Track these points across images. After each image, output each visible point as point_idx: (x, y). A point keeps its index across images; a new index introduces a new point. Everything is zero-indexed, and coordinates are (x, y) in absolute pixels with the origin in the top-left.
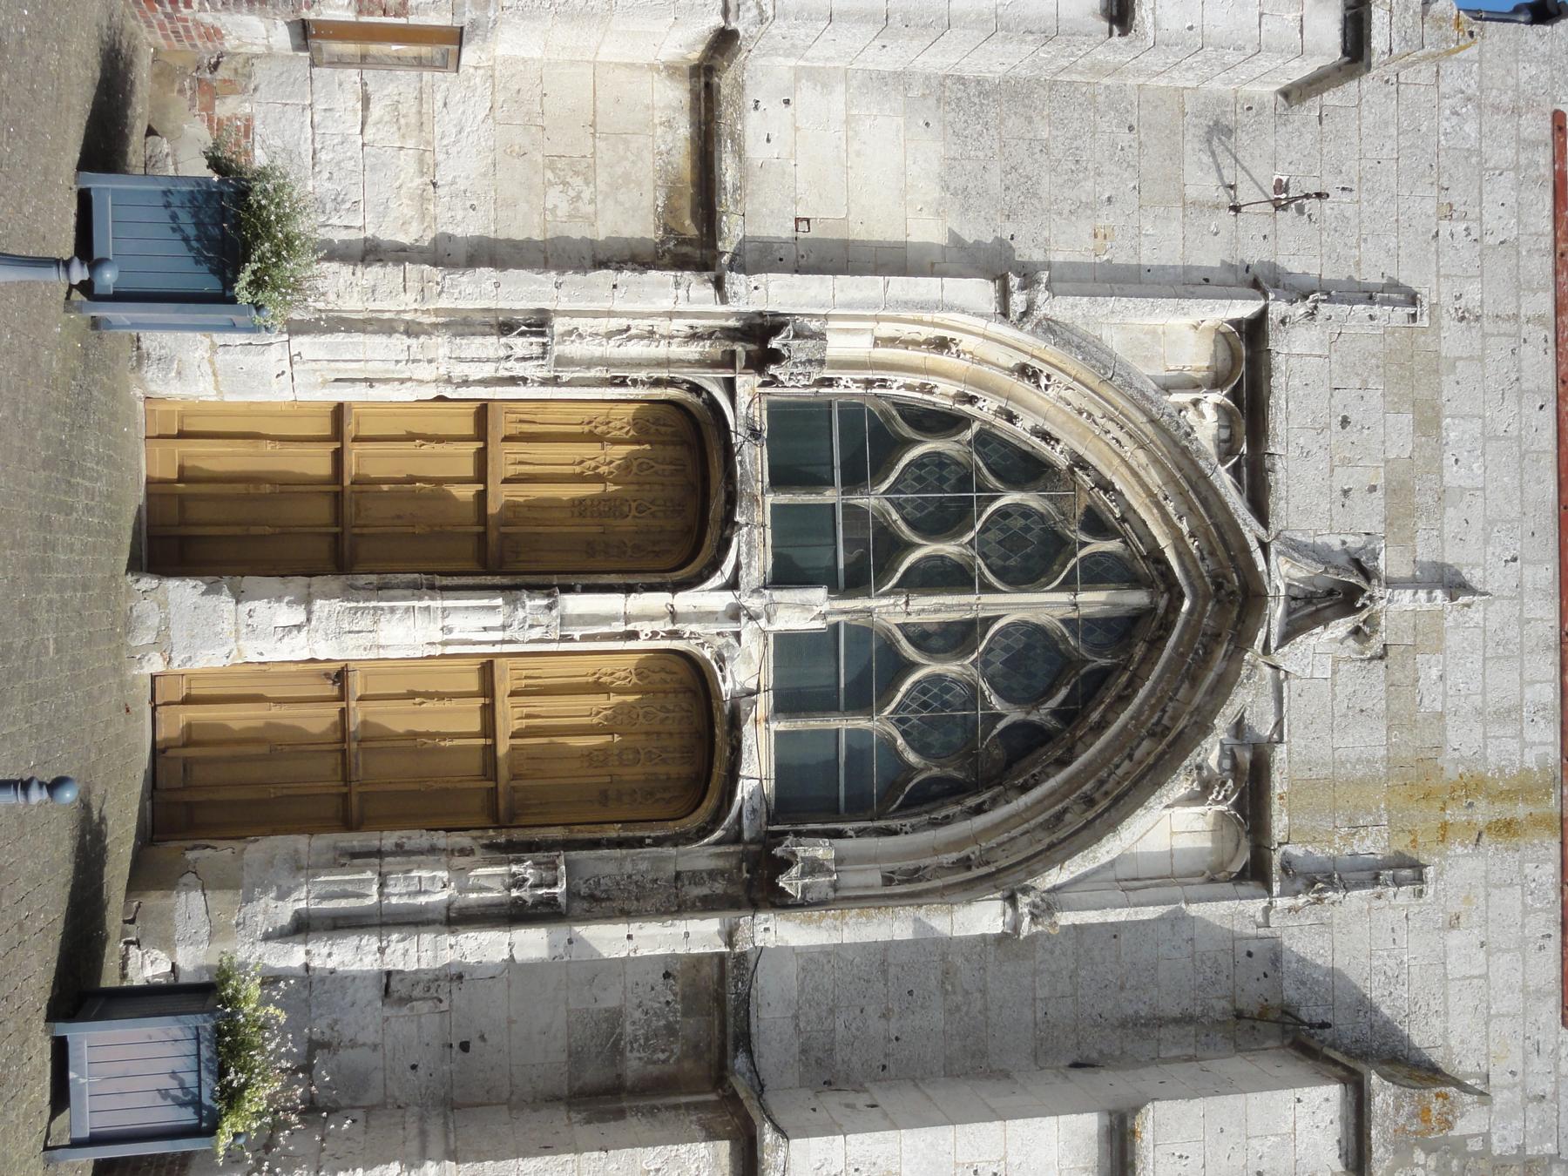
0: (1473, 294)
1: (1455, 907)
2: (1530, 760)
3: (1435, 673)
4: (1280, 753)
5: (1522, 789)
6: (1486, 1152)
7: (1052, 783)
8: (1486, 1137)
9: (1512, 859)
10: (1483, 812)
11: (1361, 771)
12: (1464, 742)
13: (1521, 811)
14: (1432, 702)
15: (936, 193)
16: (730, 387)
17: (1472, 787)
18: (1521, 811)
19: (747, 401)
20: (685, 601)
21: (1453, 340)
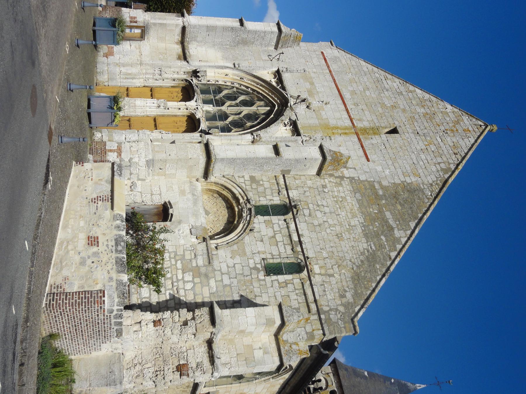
0: (315, 70)
1: (340, 144)
2: (346, 125)
3: (324, 113)
4: (298, 122)
5: (346, 128)
6: (359, 179)
7: (258, 127)
8: (358, 177)
9: (348, 138)
10: (340, 131)
11: (314, 125)
12: (333, 122)
13: (347, 131)
14: (325, 117)
15: (221, 58)
16: (192, 80)
17: (337, 128)
18: (347, 131)
19: (195, 81)
20: (188, 103)
21: (313, 75)
